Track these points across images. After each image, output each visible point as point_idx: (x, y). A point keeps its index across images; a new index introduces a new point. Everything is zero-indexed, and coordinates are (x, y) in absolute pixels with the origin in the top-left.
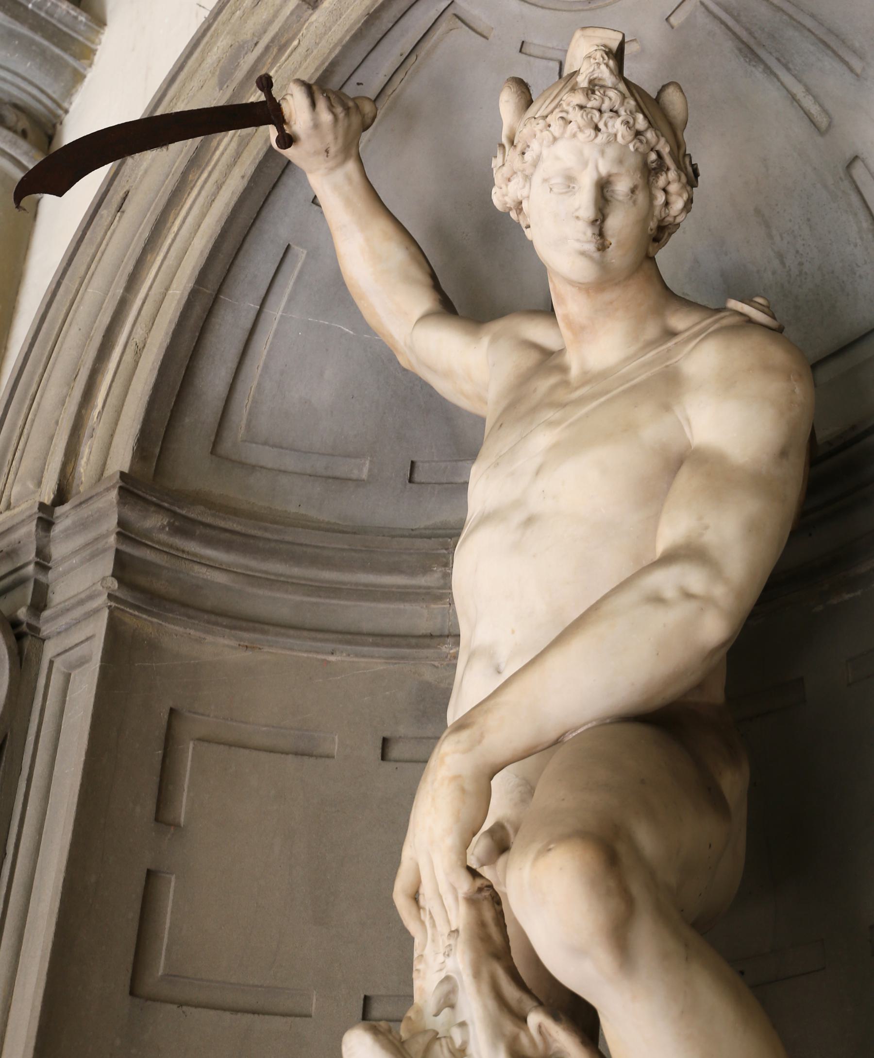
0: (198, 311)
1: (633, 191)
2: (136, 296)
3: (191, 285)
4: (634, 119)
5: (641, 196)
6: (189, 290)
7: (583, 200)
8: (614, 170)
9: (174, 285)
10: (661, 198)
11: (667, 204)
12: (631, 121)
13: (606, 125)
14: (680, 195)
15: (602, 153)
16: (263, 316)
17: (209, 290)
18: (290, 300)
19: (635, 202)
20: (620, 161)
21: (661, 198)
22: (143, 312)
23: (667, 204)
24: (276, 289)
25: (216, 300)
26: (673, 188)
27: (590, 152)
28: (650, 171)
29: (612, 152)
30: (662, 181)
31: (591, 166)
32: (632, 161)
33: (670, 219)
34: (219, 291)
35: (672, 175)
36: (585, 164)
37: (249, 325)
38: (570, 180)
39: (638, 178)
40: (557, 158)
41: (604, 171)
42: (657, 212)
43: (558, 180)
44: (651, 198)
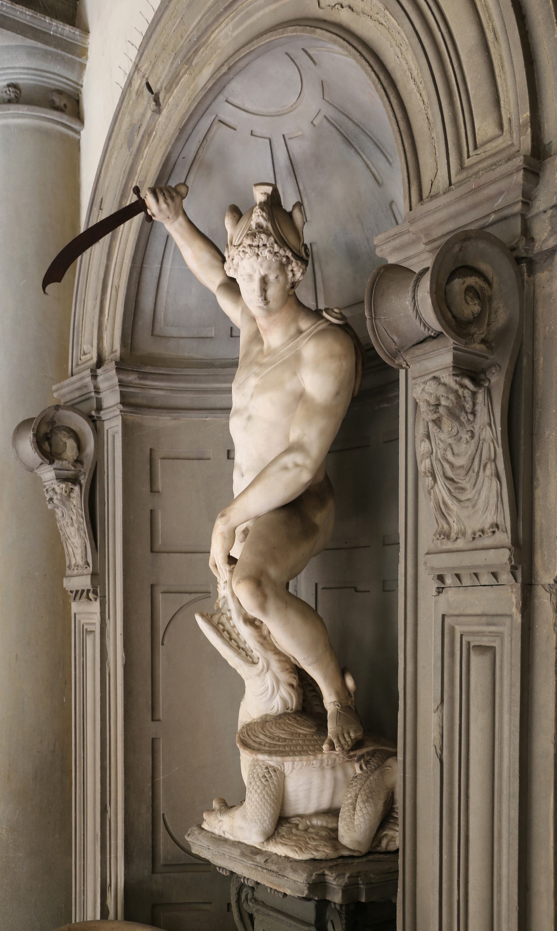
0: (135, 275)
1: (277, 278)
2: (112, 262)
3: (130, 265)
4: (273, 248)
5: (281, 278)
6: (129, 267)
7: (256, 285)
8: (267, 273)
9: (125, 258)
10: (290, 275)
11: (294, 275)
12: (272, 250)
13: (261, 253)
14: (299, 271)
15: (261, 265)
16: (163, 269)
17: (138, 265)
18: (172, 260)
19: (278, 281)
20: (269, 268)
21: (290, 275)
22: (116, 270)
23: (294, 275)
24: (166, 255)
25: (142, 267)
26: (295, 269)
27: (256, 266)
28: (283, 267)
29: (265, 265)
30: (290, 268)
31: (257, 272)
32: (275, 265)
33: (296, 280)
34: (142, 263)
35: (294, 264)
36: (255, 271)
37: (158, 275)
38: (250, 276)
39: (278, 272)
40: (244, 268)
41: (263, 273)
42: (290, 281)
43: (245, 277)
44: (286, 275)
